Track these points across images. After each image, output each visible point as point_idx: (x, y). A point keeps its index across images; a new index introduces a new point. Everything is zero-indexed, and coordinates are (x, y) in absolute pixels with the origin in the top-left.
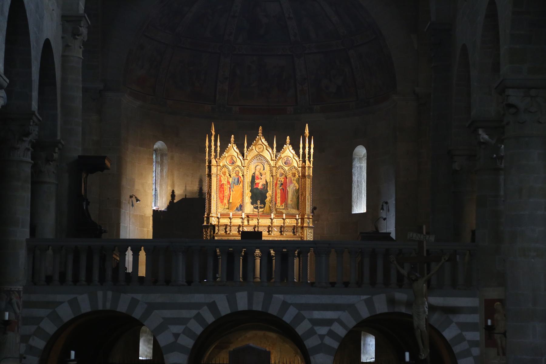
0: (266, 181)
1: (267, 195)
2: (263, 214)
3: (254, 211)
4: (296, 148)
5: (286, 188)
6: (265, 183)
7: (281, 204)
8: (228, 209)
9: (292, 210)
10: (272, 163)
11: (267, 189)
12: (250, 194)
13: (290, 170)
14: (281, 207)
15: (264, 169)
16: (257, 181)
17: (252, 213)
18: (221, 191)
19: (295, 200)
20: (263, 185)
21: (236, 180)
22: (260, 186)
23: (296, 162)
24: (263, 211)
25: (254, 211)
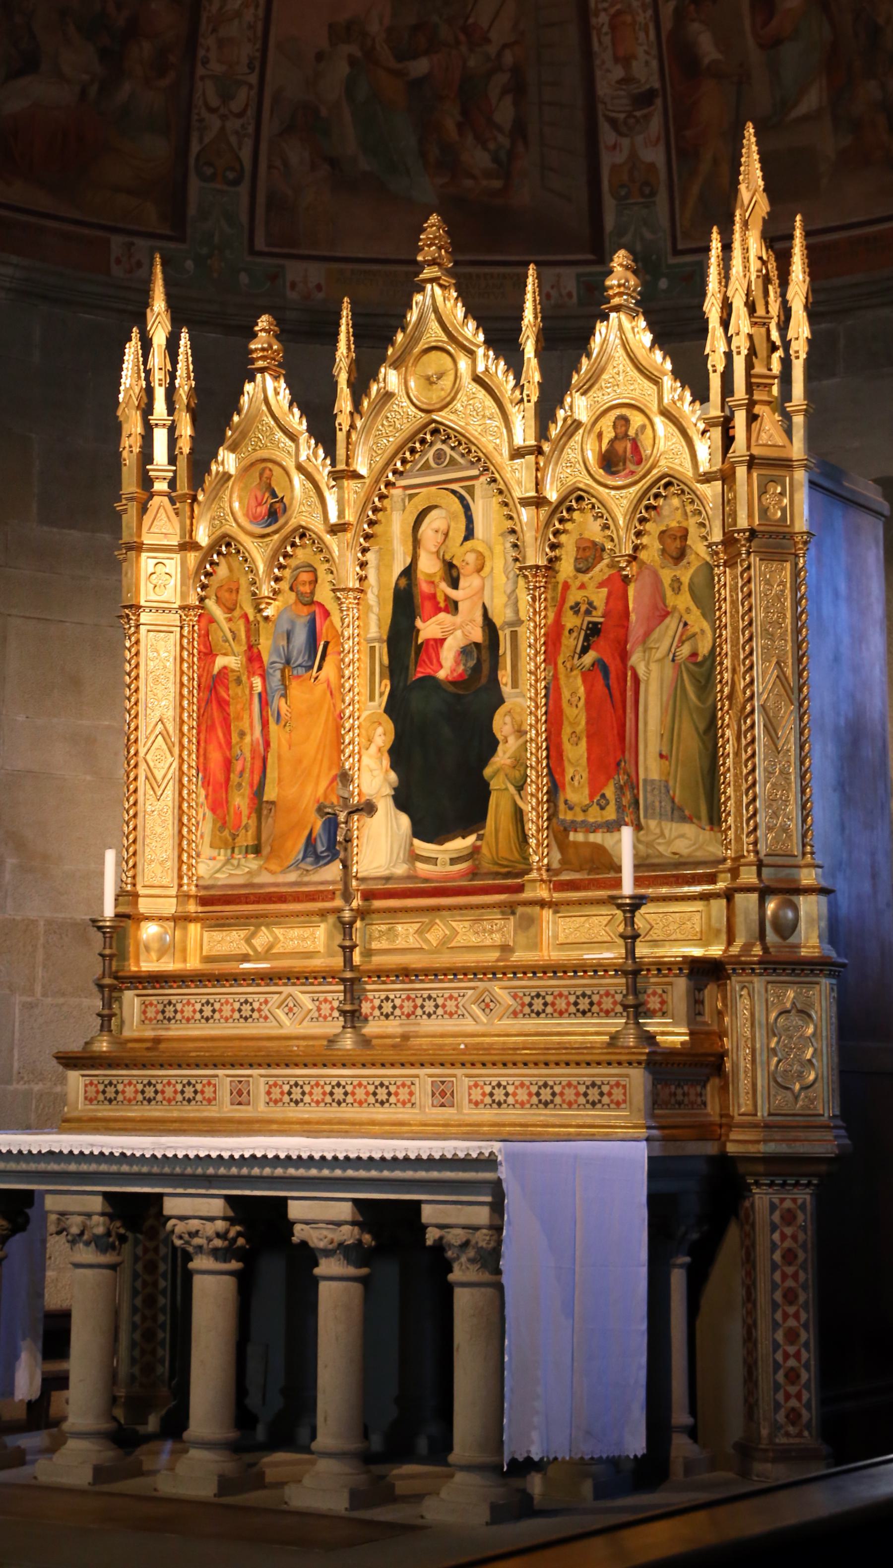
0: (489, 625)
1: (501, 725)
2: (474, 874)
3: (414, 857)
4: (678, 328)
5: (624, 656)
6: (477, 635)
7: (595, 788)
8: (257, 850)
9: (673, 829)
10: (519, 477)
11: (494, 682)
12: (383, 735)
13: (646, 509)
14: (594, 816)
15: (469, 534)
16: (428, 628)
17: (401, 870)
18: (211, 728)
19: (690, 742)
20: (465, 652)
21: (300, 638)
22: (448, 665)
23: (681, 443)
24: (475, 851)
25: (414, 857)
